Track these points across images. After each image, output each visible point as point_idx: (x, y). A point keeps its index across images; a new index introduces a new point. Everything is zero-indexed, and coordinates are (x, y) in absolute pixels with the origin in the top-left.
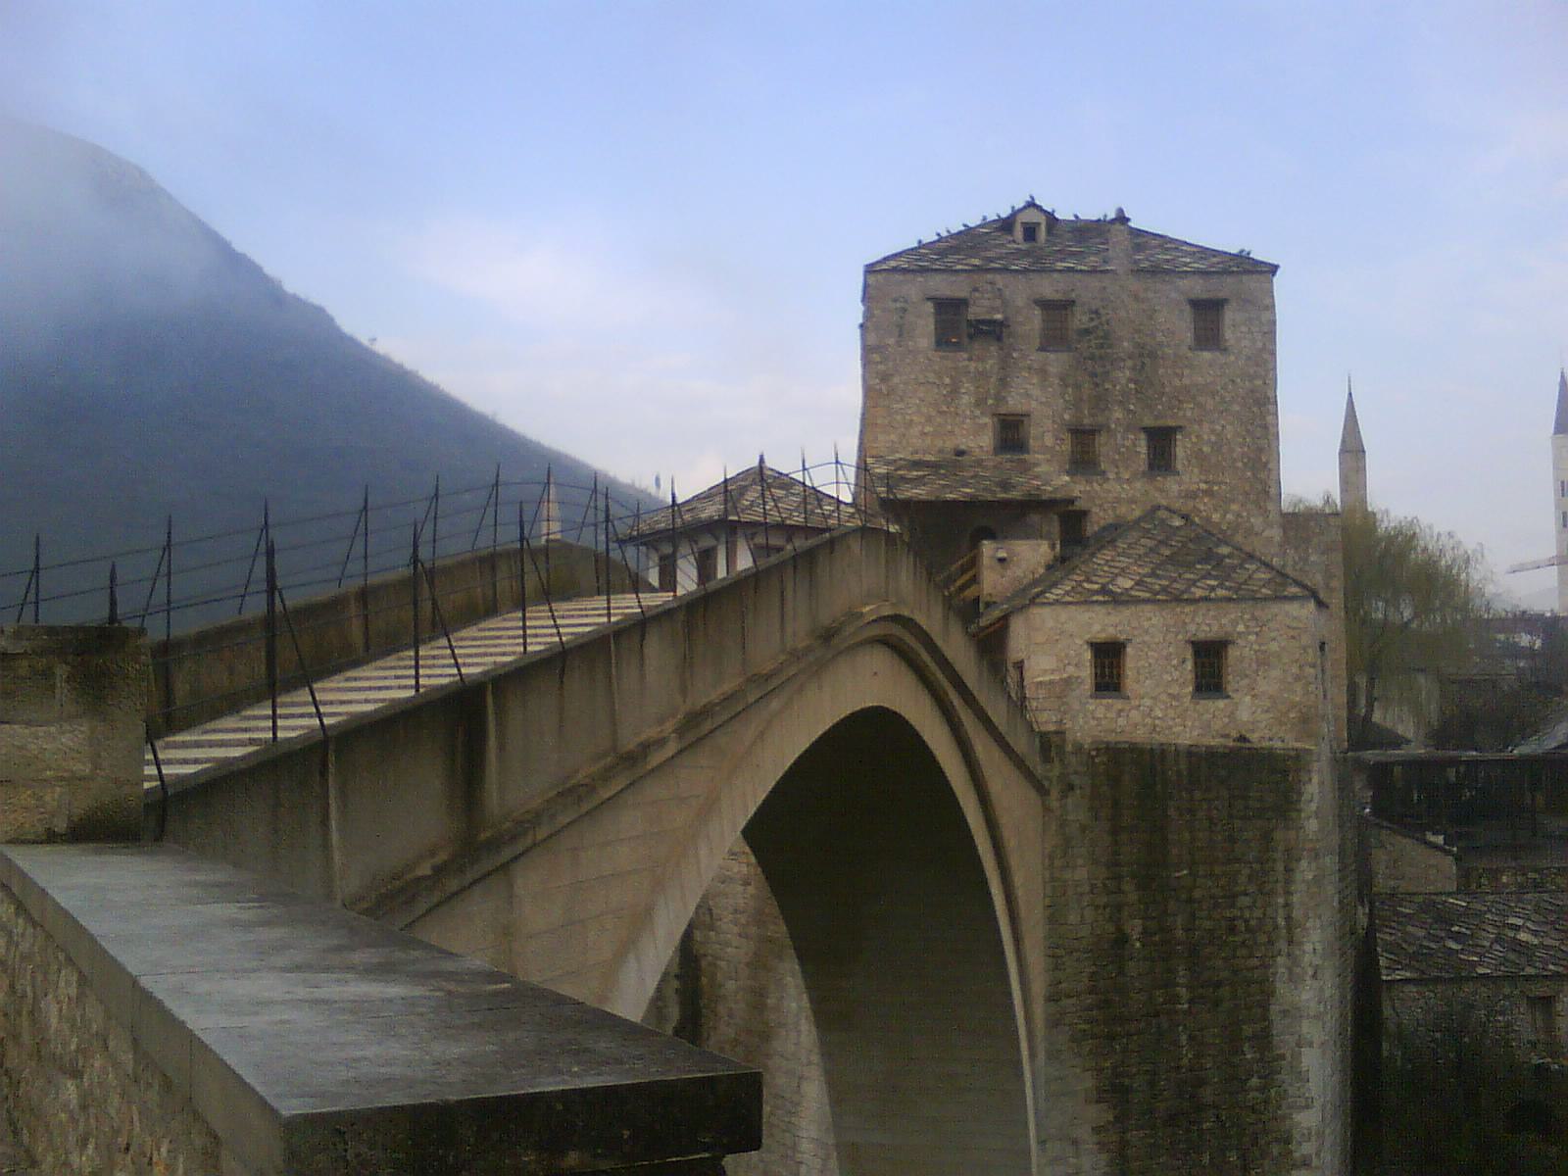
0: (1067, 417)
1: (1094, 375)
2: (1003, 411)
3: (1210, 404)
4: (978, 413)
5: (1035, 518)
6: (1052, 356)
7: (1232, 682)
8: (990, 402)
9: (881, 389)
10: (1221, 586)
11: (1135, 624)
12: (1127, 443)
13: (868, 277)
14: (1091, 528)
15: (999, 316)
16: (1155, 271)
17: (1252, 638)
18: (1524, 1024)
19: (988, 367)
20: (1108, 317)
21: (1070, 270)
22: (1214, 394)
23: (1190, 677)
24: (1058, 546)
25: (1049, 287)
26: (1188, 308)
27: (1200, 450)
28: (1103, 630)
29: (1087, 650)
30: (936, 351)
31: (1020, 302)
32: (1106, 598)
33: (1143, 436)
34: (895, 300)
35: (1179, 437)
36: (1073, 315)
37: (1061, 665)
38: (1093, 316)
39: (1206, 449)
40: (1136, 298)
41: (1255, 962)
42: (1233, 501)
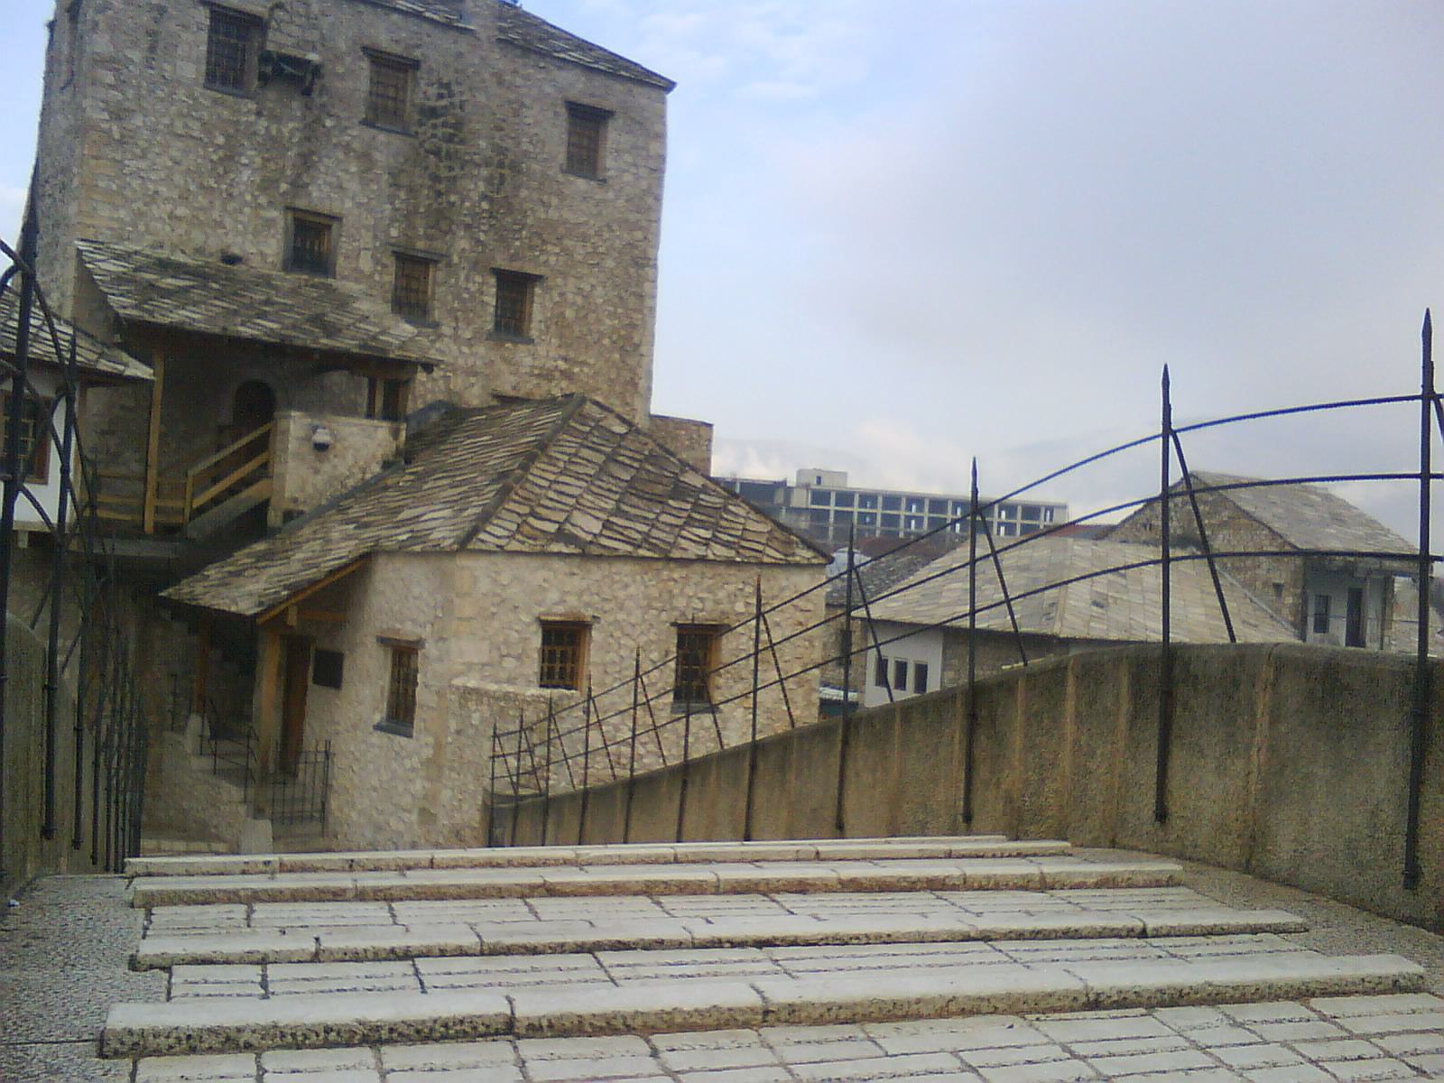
1: (436, 178)
2: (301, 203)
3: (579, 254)
4: (263, 200)
5: (337, 379)
6: (382, 137)
8: (284, 187)
9: (110, 129)
10: (715, 539)
11: (607, 593)
12: (473, 288)
15: (313, 57)
16: (527, 50)
19: (285, 131)
20: (464, 98)
22: (584, 238)
25: (386, 33)
26: (563, 111)
27: (563, 314)
28: (563, 601)
29: (536, 633)
30: (205, 87)
31: (343, 46)
33: (493, 281)
35: (538, 290)
36: (416, 83)
37: (495, 654)
38: (444, 92)
39: (569, 313)
40: (499, 79)
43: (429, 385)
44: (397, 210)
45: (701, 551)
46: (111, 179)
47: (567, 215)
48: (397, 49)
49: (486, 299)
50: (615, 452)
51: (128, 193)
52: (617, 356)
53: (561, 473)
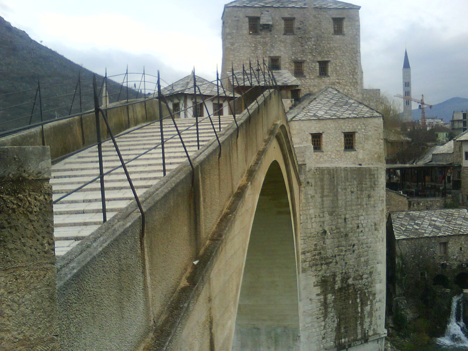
0: (293, 57)
2: (272, 55)
3: (339, 53)
6: (288, 37)
7: (357, 145)
11: (325, 127)
13: (226, 8)
14: (301, 96)
15: (271, 23)
17: (363, 130)
18: (438, 250)
21: (294, 7)
22: (340, 50)
23: (343, 144)
24: (293, 102)
26: (331, 20)
31: (277, 18)
32: (316, 118)
33: (318, 64)
34: (235, 17)
35: (329, 64)
37: (301, 141)
39: (338, 68)
41: (365, 237)
42: (346, 85)
43: (305, 90)
44: (293, 52)
45: (348, 116)
46: (233, 58)
47: (336, 45)
48: (289, 16)
49: (316, 68)
50: (333, 97)
51: (236, 60)
52: (351, 76)
53: (318, 103)
